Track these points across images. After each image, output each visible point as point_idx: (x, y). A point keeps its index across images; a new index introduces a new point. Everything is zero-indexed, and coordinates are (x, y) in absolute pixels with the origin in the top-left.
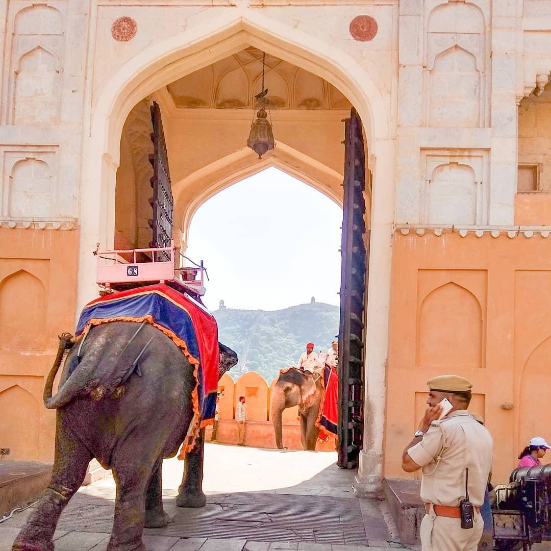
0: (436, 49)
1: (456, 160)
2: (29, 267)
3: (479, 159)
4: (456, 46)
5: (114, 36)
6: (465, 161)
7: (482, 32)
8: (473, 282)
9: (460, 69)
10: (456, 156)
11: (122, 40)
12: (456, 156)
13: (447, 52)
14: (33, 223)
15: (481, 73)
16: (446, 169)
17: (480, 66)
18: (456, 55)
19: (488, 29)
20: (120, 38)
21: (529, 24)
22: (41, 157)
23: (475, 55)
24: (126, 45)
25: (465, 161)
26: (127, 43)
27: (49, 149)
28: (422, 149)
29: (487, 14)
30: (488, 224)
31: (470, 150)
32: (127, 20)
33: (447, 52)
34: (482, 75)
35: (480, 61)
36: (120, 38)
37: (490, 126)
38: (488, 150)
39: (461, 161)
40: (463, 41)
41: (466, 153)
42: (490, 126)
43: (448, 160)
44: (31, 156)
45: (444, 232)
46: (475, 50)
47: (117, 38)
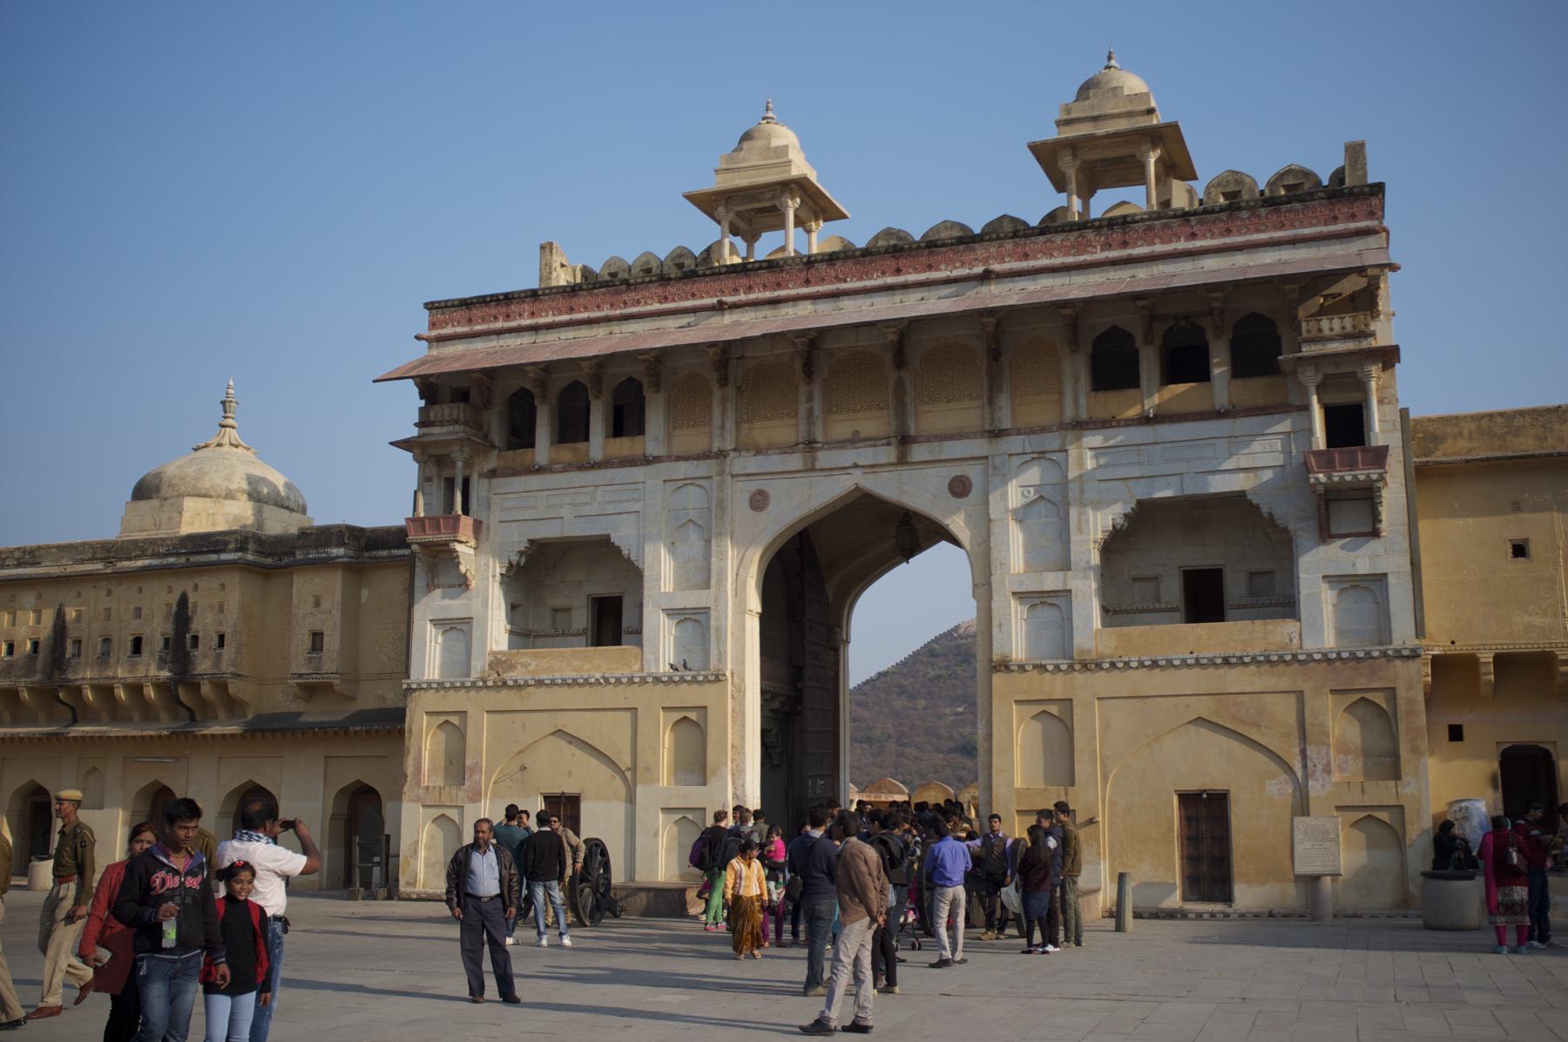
6: (1053, 600)
18: (1042, 503)
24: (762, 515)
25: (1053, 600)
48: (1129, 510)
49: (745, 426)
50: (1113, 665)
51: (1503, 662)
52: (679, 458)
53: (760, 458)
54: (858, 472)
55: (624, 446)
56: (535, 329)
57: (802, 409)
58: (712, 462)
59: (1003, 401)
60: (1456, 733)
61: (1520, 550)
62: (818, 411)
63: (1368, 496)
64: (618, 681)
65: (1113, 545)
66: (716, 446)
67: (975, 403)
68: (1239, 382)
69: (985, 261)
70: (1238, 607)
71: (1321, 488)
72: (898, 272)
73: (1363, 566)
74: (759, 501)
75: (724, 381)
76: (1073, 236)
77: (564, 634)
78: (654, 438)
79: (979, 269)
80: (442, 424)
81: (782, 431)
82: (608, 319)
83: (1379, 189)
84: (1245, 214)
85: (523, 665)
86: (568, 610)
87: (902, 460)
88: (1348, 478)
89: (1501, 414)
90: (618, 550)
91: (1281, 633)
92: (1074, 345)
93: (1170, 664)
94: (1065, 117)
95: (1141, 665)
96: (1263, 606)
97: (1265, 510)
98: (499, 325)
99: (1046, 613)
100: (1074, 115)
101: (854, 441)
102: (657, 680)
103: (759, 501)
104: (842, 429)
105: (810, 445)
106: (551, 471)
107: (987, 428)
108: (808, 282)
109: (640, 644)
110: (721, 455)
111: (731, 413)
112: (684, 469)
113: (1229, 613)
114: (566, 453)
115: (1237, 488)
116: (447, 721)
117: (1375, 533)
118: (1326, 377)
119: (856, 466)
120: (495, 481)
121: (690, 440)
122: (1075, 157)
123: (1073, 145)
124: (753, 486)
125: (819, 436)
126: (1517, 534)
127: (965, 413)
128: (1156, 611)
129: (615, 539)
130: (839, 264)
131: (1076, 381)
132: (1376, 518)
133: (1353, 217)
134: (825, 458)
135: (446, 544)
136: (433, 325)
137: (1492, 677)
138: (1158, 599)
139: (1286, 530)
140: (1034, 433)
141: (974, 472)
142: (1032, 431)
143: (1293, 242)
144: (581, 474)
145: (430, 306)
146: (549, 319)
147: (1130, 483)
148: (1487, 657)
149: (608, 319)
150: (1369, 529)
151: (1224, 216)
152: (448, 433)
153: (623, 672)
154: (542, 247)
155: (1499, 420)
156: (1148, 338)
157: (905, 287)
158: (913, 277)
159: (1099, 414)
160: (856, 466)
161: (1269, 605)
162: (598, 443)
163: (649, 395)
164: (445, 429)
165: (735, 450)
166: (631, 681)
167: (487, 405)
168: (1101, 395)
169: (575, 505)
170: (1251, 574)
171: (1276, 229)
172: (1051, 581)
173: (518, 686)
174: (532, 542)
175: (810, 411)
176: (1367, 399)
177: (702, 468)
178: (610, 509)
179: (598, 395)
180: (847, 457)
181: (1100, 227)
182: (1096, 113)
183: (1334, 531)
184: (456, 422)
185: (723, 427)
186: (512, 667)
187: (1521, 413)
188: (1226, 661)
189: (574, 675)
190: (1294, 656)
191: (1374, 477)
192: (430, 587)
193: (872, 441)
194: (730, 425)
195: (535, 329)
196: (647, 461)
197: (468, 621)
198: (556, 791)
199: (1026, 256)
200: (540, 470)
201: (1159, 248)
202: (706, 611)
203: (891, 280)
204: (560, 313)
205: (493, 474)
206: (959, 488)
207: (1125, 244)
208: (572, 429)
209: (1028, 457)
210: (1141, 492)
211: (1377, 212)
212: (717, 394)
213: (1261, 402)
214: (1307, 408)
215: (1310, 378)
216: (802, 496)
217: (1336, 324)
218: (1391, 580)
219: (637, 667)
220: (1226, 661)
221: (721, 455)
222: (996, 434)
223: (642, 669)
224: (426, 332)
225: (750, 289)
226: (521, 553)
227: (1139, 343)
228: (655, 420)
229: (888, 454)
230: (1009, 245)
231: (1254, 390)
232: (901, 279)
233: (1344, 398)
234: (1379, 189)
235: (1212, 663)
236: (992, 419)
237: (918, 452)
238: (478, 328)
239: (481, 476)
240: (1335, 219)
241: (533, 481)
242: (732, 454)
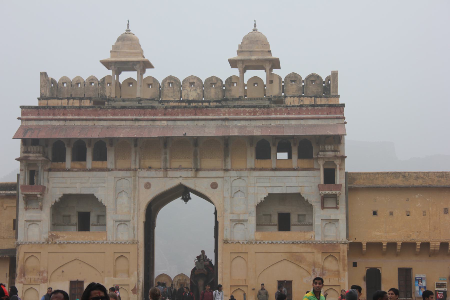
0: (234, 191)
2: (124, 255)
6: (242, 223)
10: (240, 222)
12: (240, 222)
14: (125, 242)
16: (238, 225)
18: (240, 192)
21: (258, 185)
22: (126, 223)
24: (148, 190)
33: (237, 192)
43: (238, 222)
45: (236, 243)
48: (266, 196)
50: (260, 243)
51: (368, 244)
53: (149, 172)
54: (181, 179)
55: (99, 164)
56: (65, 120)
57: (163, 157)
58: (132, 172)
59: (229, 160)
60: (355, 264)
61: (375, 213)
62: (168, 158)
63: (335, 197)
64: (98, 243)
65: (259, 207)
66: (133, 167)
68: (300, 160)
69: (224, 114)
70: (295, 225)
71: (323, 195)
72: (196, 114)
73: (333, 218)
74: (148, 186)
75: (136, 146)
76: (252, 109)
77: (68, 225)
78: (110, 163)
79: (222, 117)
80: (34, 153)
81: (155, 163)
82: (93, 120)
83: (343, 105)
84: (304, 109)
85: (62, 237)
86: (69, 216)
87: (196, 177)
88: (330, 193)
89: (373, 173)
90: (97, 198)
91: (309, 235)
92: (251, 145)
93: (277, 243)
94: (241, 50)
96: (302, 225)
97: (306, 199)
98: (51, 117)
99: (239, 226)
100: (243, 50)
101: (180, 169)
102: (112, 243)
104: (176, 164)
105: (166, 169)
106: (72, 171)
107: (223, 168)
108: (165, 115)
109: (105, 230)
110: (135, 170)
111: (138, 156)
112: (122, 174)
113: (292, 228)
114: (77, 165)
115: (298, 192)
116: (32, 256)
117: (337, 208)
118: (326, 162)
119: (181, 177)
120: (51, 173)
121: (122, 163)
122: (243, 64)
123: (243, 61)
124: (146, 181)
125: (168, 166)
126: (375, 209)
127: (218, 162)
128: (270, 225)
129: (96, 195)
130: (175, 110)
131: (252, 156)
132: (337, 203)
133: (335, 113)
134: (170, 174)
135: (37, 195)
136: (23, 114)
137: (365, 249)
138: (271, 221)
139: (311, 206)
140: (238, 171)
141: (219, 182)
142: (237, 170)
143: (318, 119)
144: (84, 173)
145: (22, 107)
146: (71, 117)
147: (267, 188)
148: (364, 244)
149: (93, 120)
150: (335, 206)
151: (298, 108)
152: (37, 157)
154: (42, 74)
155: (372, 175)
156: (274, 145)
157: (198, 120)
158: (201, 117)
159: (258, 166)
160: (181, 177)
161: (304, 225)
162: (89, 163)
163: (108, 147)
164: (34, 155)
165: (139, 168)
166: (103, 243)
167: (47, 146)
168: (259, 161)
169: (82, 183)
170: (299, 215)
171: (314, 114)
173: (60, 244)
174: (64, 194)
175: (166, 158)
176: (336, 168)
177: (128, 174)
178: (94, 185)
179: (90, 145)
180: (178, 174)
181: (261, 107)
182: (251, 50)
183: (325, 206)
184: (39, 152)
185: (135, 161)
186: (58, 237)
187: (378, 173)
188: (293, 243)
189: (82, 241)
190: (312, 242)
191: (337, 193)
192: (26, 209)
193: (186, 169)
194: (138, 160)
195: (65, 120)
196: (109, 170)
197: (40, 221)
198: (75, 279)
199: (237, 114)
200: (69, 170)
201: (278, 116)
203: (193, 117)
204: (75, 116)
205: (50, 170)
206: (214, 186)
207: (268, 114)
208: (79, 156)
209: (236, 178)
210: (270, 191)
211: (342, 112)
212: (133, 149)
213: (306, 167)
214: (319, 169)
215: (321, 163)
216: (161, 185)
217: (329, 147)
218: (340, 221)
219: (105, 239)
220: (293, 243)
221: (135, 170)
222: (226, 170)
223: (106, 240)
224: (20, 116)
225: (144, 115)
226: (59, 198)
227: (271, 145)
228: (111, 156)
229: (191, 174)
230: (232, 110)
231: (305, 163)
232: (197, 117)
233: (330, 167)
234: (343, 105)
235: (289, 243)
236: (225, 166)
237: (201, 174)
238: (42, 117)
239: (45, 170)
240: (330, 113)
241: (65, 174)
242: (139, 170)
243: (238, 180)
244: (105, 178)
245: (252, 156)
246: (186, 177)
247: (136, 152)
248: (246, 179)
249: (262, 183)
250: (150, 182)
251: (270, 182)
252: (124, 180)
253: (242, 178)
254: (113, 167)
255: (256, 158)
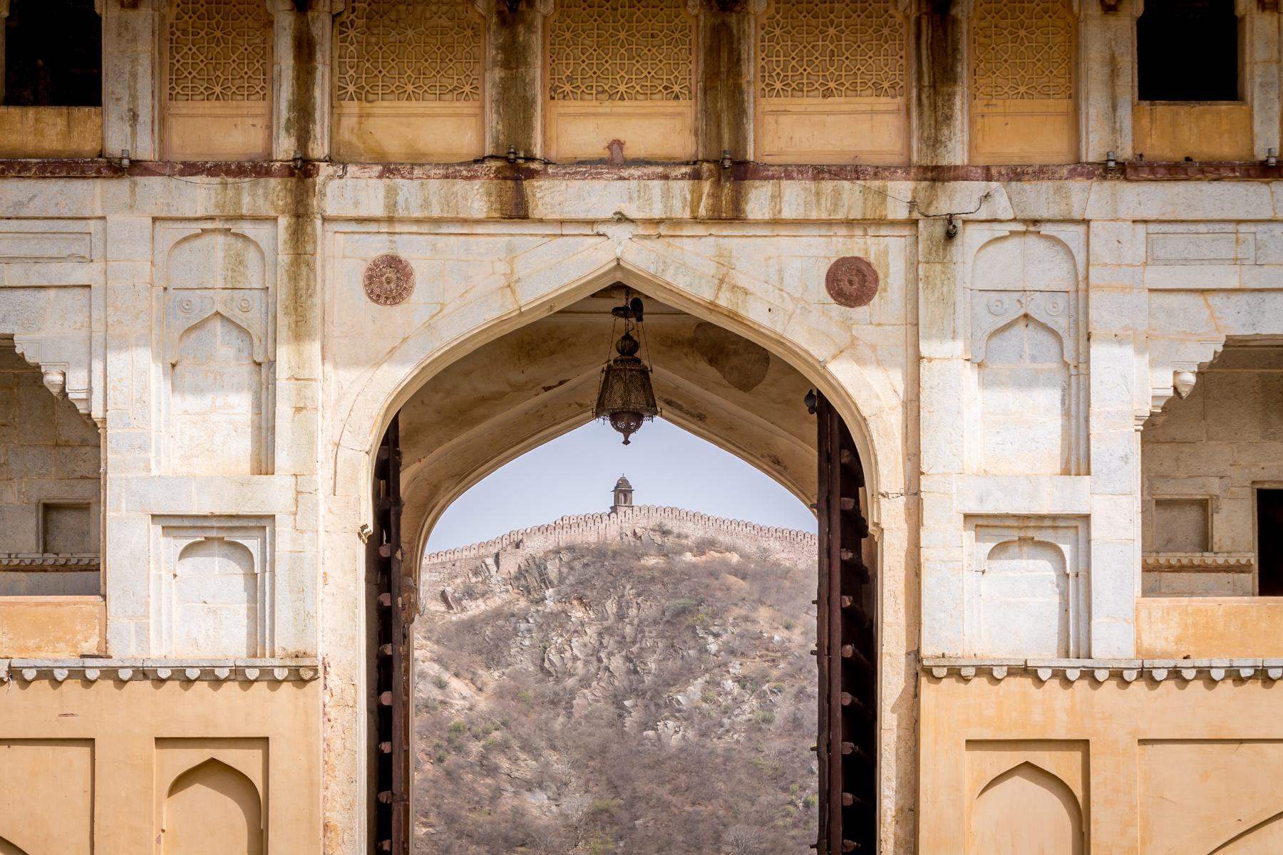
1: (1030, 533)
3: (1072, 531)
4: (1026, 316)
5: (370, 294)
7: (1072, 288)
8: (1064, 765)
9: (1034, 359)
11: (385, 304)
13: (1010, 325)
15: (1072, 367)
17: (1069, 356)
19: (1082, 286)
20: (382, 300)
23: (1060, 332)
26: (395, 307)
27: (252, 523)
28: (967, 516)
29: (1080, 258)
30: (1090, 657)
31: (1054, 518)
32: (393, 262)
33: (1010, 325)
34: (1073, 371)
35: (1068, 344)
36: (382, 300)
37: (1089, 473)
38: (1086, 518)
39: (1039, 536)
40: (1038, 307)
41: (1047, 523)
42: (1089, 473)
43: (1014, 535)
44: (214, 534)
45: (1013, 672)
46: (1061, 323)
47: (375, 297)
49: (351, 107)
52: (191, 169)
64: (45, 674)
67: (885, 103)
95: (1234, 675)
102: (143, 673)
103: (389, 282)
119: (621, 218)
124: (376, 246)
147: (1216, 300)
153: (62, 656)
159: (1159, 148)
160: (621, 218)
165: (330, 160)
166: (77, 674)
172: (1054, 496)
180: (603, 196)
193: (660, 166)
202: (262, 523)
209: (1003, 230)
222: (937, 175)
243: (1015, 243)
244: (92, 226)
245: (1114, 73)
246: (658, 222)
247: (305, 49)
248: (1072, 235)
249: (1186, 261)
250: (403, 255)
251: (1235, 261)
252: (220, 239)
253: (1046, 229)
254: (145, 149)
255: (1142, 97)
